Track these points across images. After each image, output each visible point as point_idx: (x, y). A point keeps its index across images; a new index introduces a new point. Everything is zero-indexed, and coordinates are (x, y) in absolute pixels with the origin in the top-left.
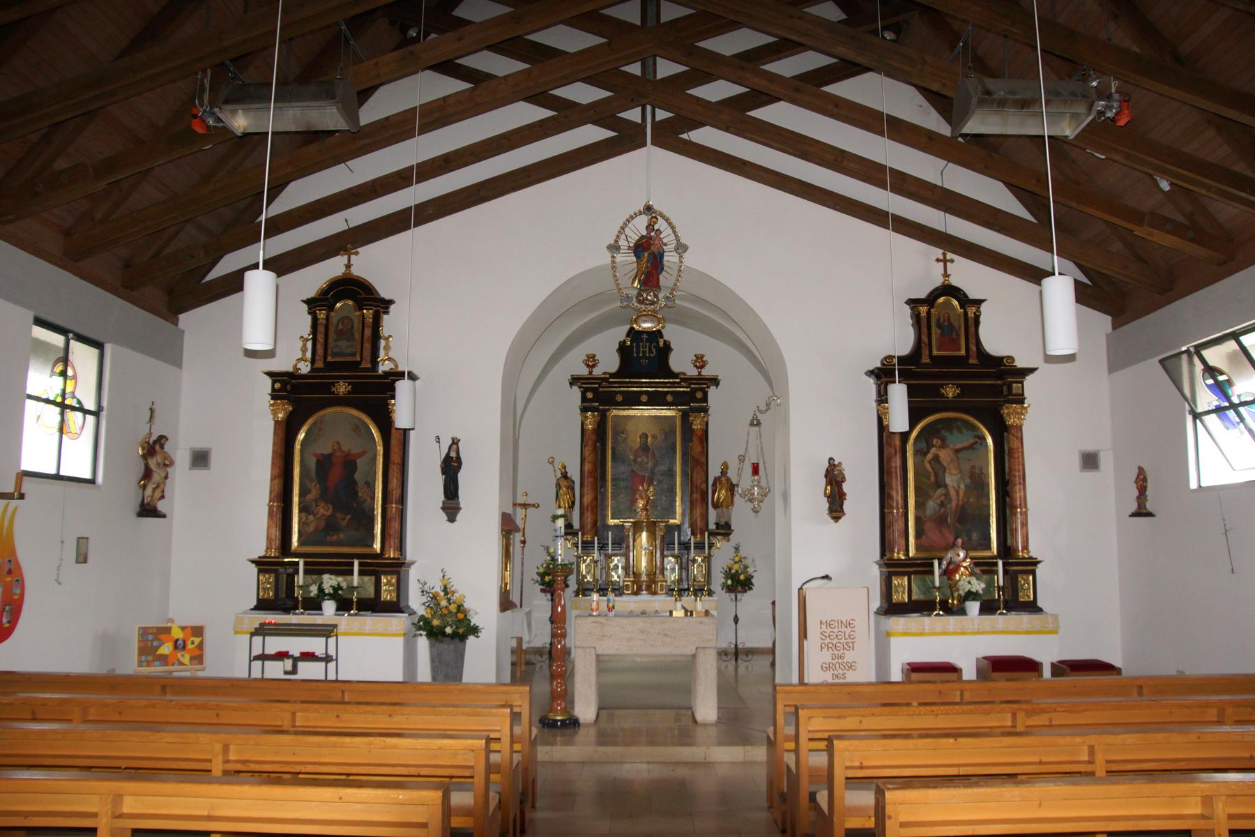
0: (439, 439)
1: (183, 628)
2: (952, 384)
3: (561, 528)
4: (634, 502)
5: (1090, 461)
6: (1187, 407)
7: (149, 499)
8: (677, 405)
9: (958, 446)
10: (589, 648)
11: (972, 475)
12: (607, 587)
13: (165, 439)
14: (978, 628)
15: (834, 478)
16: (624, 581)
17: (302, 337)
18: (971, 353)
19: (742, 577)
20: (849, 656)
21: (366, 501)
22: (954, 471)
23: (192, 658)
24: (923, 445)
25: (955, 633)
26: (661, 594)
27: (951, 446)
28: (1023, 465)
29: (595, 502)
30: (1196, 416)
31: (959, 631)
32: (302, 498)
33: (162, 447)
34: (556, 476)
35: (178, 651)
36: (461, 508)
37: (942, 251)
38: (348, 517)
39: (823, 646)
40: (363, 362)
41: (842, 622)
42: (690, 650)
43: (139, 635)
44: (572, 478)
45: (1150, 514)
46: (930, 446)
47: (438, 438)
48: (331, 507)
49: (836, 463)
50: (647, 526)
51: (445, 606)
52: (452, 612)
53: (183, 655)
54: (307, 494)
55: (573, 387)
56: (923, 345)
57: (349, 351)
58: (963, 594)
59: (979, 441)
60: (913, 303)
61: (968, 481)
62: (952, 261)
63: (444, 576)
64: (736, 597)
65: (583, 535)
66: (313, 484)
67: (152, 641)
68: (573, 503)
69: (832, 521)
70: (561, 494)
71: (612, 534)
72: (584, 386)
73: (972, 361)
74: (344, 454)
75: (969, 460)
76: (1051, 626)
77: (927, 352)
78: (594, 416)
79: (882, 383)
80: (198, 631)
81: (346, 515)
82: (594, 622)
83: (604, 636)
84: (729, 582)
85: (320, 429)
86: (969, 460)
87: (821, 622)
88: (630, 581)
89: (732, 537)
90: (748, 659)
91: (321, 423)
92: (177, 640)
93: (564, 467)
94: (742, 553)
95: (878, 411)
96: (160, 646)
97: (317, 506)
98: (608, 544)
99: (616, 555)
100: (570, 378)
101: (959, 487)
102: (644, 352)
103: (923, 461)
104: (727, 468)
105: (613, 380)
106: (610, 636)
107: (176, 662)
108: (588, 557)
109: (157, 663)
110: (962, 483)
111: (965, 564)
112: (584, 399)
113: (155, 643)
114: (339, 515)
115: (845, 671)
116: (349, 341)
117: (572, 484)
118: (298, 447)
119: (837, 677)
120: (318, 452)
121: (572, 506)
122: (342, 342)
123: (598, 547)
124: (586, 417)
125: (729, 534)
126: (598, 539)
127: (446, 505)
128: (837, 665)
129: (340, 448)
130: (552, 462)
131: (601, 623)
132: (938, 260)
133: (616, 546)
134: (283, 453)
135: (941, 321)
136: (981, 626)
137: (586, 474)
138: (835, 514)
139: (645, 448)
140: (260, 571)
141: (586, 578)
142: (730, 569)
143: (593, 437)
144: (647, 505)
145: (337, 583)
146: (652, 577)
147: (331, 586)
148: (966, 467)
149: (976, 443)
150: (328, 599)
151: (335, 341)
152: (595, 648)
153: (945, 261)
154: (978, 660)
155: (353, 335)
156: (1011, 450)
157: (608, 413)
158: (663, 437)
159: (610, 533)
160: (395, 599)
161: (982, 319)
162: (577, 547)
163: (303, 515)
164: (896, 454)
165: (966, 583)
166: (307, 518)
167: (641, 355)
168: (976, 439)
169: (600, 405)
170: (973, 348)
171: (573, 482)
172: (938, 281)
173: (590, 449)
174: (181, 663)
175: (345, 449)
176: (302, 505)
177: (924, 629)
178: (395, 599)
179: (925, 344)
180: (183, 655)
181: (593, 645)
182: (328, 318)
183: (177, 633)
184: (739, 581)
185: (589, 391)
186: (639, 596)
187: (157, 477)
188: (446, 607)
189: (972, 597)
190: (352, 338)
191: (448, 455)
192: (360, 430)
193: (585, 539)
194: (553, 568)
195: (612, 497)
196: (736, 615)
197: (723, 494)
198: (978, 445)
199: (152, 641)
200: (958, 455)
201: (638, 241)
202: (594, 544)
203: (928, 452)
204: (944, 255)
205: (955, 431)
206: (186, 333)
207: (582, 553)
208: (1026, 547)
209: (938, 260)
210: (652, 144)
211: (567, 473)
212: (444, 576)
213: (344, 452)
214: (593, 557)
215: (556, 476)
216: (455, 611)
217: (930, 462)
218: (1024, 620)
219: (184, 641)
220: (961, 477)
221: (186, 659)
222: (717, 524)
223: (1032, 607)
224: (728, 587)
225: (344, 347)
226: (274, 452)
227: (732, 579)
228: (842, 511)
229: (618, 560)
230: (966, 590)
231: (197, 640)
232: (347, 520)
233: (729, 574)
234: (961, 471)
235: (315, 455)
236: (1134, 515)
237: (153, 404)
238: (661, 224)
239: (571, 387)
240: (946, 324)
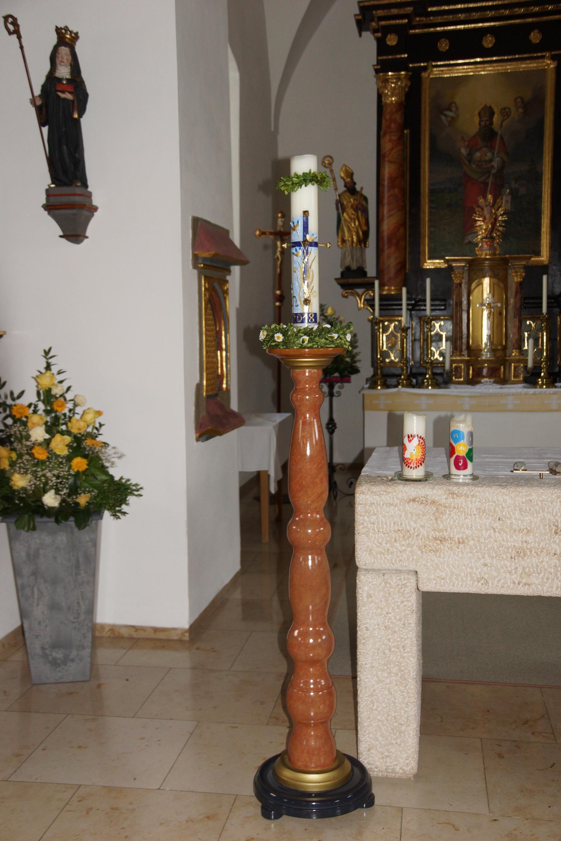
0: (15, 23)
3: (306, 213)
4: (470, 227)
8: (550, 50)
10: (399, 572)
12: (423, 370)
16: (452, 362)
26: (514, 383)
29: (401, 230)
34: (336, 189)
36: (95, 209)
44: (364, 193)
50: (492, 268)
51: (40, 439)
52: (58, 456)
55: (364, 33)
65: (381, 286)
68: (366, 234)
70: (345, 220)
71: (432, 283)
72: (383, 23)
78: (399, 79)
83: (442, 540)
88: (461, 361)
93: (350, 175)
98: (425, 300)
99: (437, 319)
100: (357, 12)
105: (434, 9)
108: (391, 322)
112: (382, 48)
117: (364, 203)
121: (363, 240)
123: (408, 305)
124: (386, 81)
126: (408, 292)
127: (53, 200)
130: (330, 164)
131: (433, 502)
133: (437, 303)
137: (386, 183)
141: (389, 357)
143: (398, 117)
144: (492, 231)
146: (499, 354)
152: (416, 572)
157: (424, 75)
159: (428, 281)
162: (373, 306)
169: (410, 60)
171: (366, 199)
173: (394, 138)
181: (412, 567)
185: (391, 33)
186: (478, 386)
188: (47, 442)
191: (52, 79)
193: (385, 293)
194: (284, 343)
195: (430, 220)
202: (401, 300)
207: (381, 315)
214: (400, 322)
215: (336, 189)
229: (440, 326)
239: (360, 35)
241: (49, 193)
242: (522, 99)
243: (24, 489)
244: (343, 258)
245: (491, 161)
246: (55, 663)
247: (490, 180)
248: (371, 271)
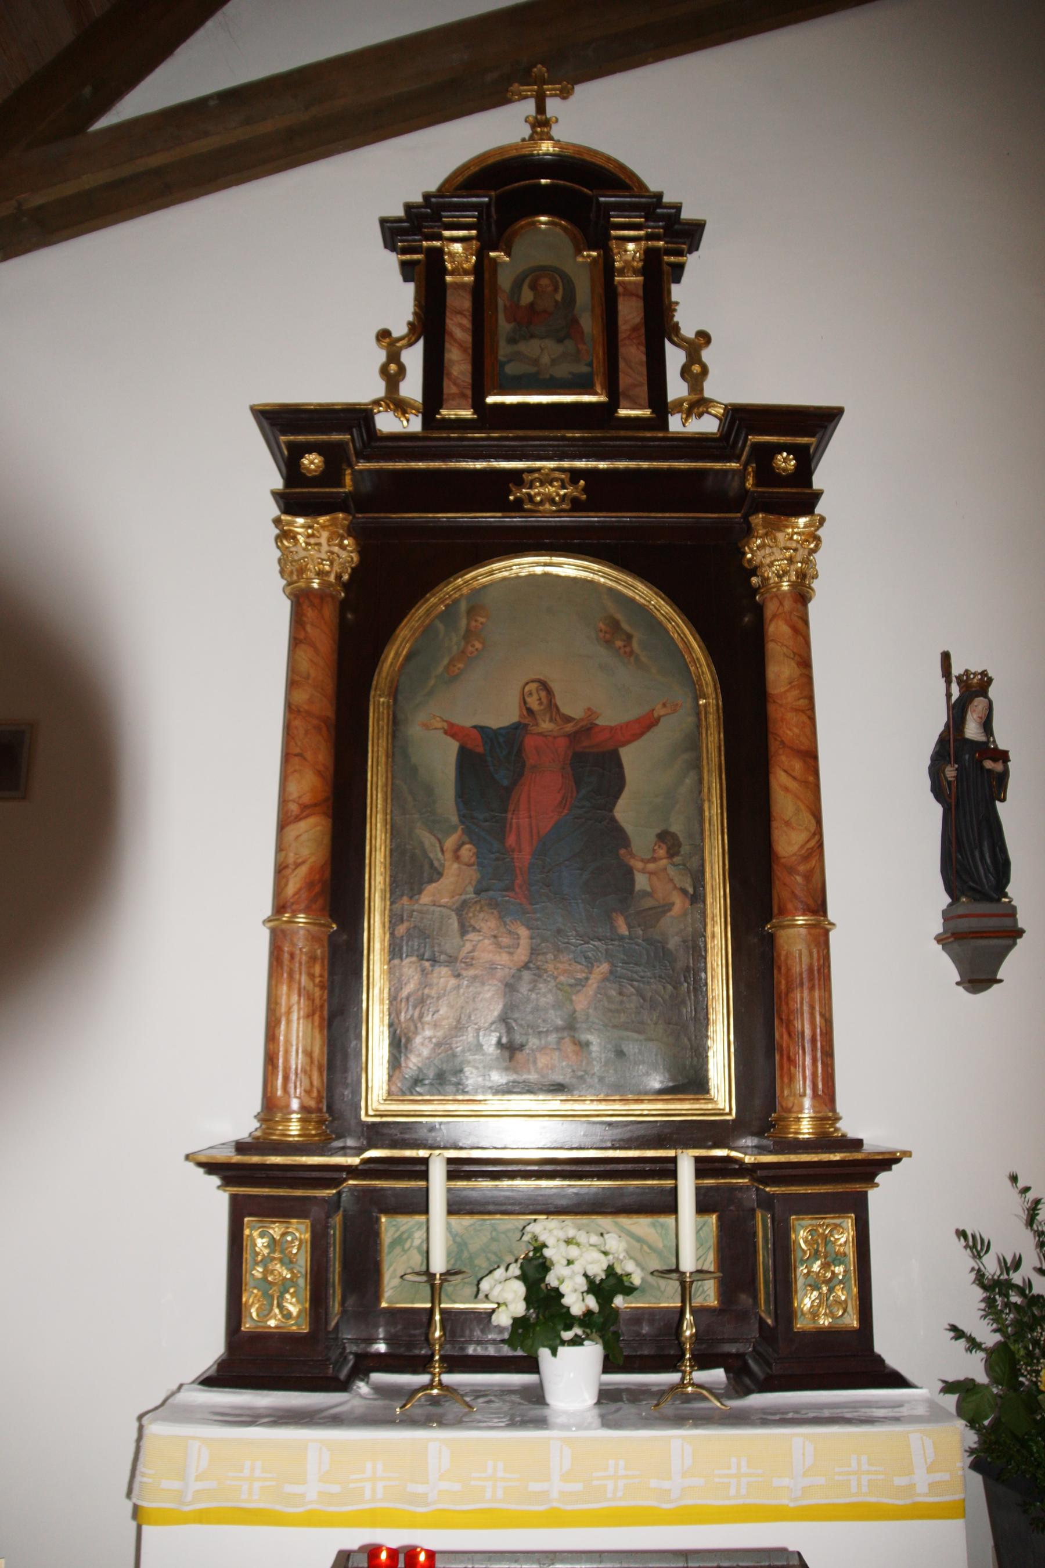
17: (384, 335)
21: (673, 904)
66: (450, 842)
74: (569, 728)
85: (469, 635)
91: (472, 612)
97: (464, 929)
116: (560, 341)
120: (466, 721)
122: (535, 343)
129: (551, 706)
134: (330, 713)
140: (238, 1212)
150: (576, 1342)
151: (512, 341)
155: (575, 321)
160: (852, 1321)
166: (425, 984)
175: (573, 707)
178: (852, 1321)
182: (483, 269)
190: (570, 330)
192: (629, 637)
213: (568, 719)
225: (545, 360)
226: (291, 709)
235: (452, 731)
241: (948, 916)
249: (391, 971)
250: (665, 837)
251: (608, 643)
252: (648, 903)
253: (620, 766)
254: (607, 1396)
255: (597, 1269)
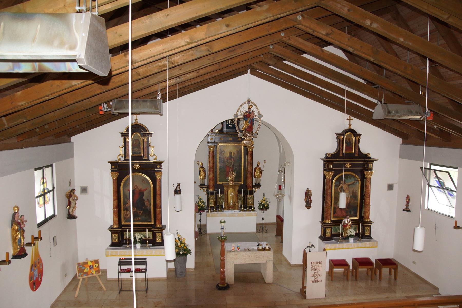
1: (92, 262)
2: (349, 163)
5: (390, 187)
6: (427, 183)
7: (72, 213)
9: (349, 183)
11: (353, 193)
13: (74, 190)
14: (353, 247)
15: (308, 195)
18: (356, 152)
19: (266, 206)
20: (320, 272)
21: (148, 206)
22: (347, 192)
23: (96, 271)
24: (338, 183)
25: (346, 248)
26: (237, 210)
27: (347, 183)
28: (370, 191)
30: (429, 186)
31: (347, 248)
32: (125, 206)
33: (74, 193)
35: (91, 270)
37: (349, 116)
38: (142, 212)
39: (312, 269)
40: (144, 156)
41: (318, 262)
42: (265, 261)
43: (77, 266)
45: (409, 211)
46: (340, 183)
47: (173, 185)
48: (135, 208)
49: (310, 190)
53: (93, 271)
54: (127, 204)
56: (340, 150)
57: (138, 152)
58: (348, 235)
59: (356, 182)
60: (338, 135)
61: (351, 195)
62: (352, 120)
63: (177, 233)
64: (263, 212)
67: (82, 268)
68: (205, 176)
69: (307, 209)
73: (356, 155)
74: (139, 190)
75: (352, 188)
76: (375, 245)
77: (342, 152)
79: (326, 164)
80: (97, 262)
81: (141, 211)
82: (233, 254)
84: (261, 207)
86: (352, 188)
87: (312, 262)
89: (260, 188)
90: (266, 232)
92: (90, 266)
94: (266, 197)
95: (324, 172)
96: (85, 269)
101: (348, 197)
102: (231, 122)
103: (337, 189)
104: (259, 164)
106: (239, 258)
107: (91, 274)
109: (85, 275)
110: (349, 195)
111: (349, 224)
113: (83, 268)
114: (138, 211)
115: (318, 277)
116: (138, 148)
118: (122, 187)
119: (316, 278)
122: (136, 149)
125: (260, 187)
128: (316, 275)
132: (348, 119)
134: (116, 190)
135: (347, 141)
136: (354, 246)
138: (308, 208)
139: (231, 157)
140: (112, 233)
142: (261, 203)
145: (141, 237)
147: (139, 238)
148: (351, 190)
149: (355, 182)
150: (138, 243)
152: (234, 262)
153: (350, 120)
154: (353, 258)
156: (366, 186)
158: (237, 153)
161: (361, 141)
163: (125, 211)
164: (329, 188)
165: (350, 232)
166: (127, 213)
167: (229, 123)
168: (355, 181)
170: (357, 151)
171: (205, 169)
172: (347, 127)
174: (92, 274)
175: (139, 188)
176: (124, 208)
177: (336, 248)
179: (341, 149)
180: (93, 271)
183: (90, 264)
184: (265, 207)
187: (73, 204)
188: (180, 245)
189: (351, 237)
192: (144, 181)
196: (263, 217)
197: (257, 173)
198: (356, 183)
199: (82, 268)
200: (349, 186)
201: (244, 114)
203: (339, 185)
204: (350, 117)
205: (349, 178)
206: (74, 143)
208: (368, 218)
209: (348, 119)
210: (250, 74)
211: (203, 166)
212: (177, 233)
213: (139, 189)
216: (183, 246)
217: (340, 189)
218: (366, 244)
219: (93, 266)
220: (349, 194)
221: (94, 272)
222: (255, 184)
223: (369, 237)
224: (261, 208)
225: (137, 151)
227: (262, 206)
228: (310, 207)
230: (350, 234)
231: (97, 265)
232: (141, 213)
233: (260, 204)
234: (349, 192)
236: (404, 210)
237: (70, 180)
238: (253, 108)
240: (349, 142)
242: (237, 151)
243: (178, 251)
244: (200, 182)
245: (231, 162)
246: (180, 275)
247: (231, 166)
248: (206, 184)
249: (124, 212)
250: (148, 200)
251: (143, 182)
252: (146, 206)
253: (144, 193)
254: (141, 247)
255: (140, 237)
